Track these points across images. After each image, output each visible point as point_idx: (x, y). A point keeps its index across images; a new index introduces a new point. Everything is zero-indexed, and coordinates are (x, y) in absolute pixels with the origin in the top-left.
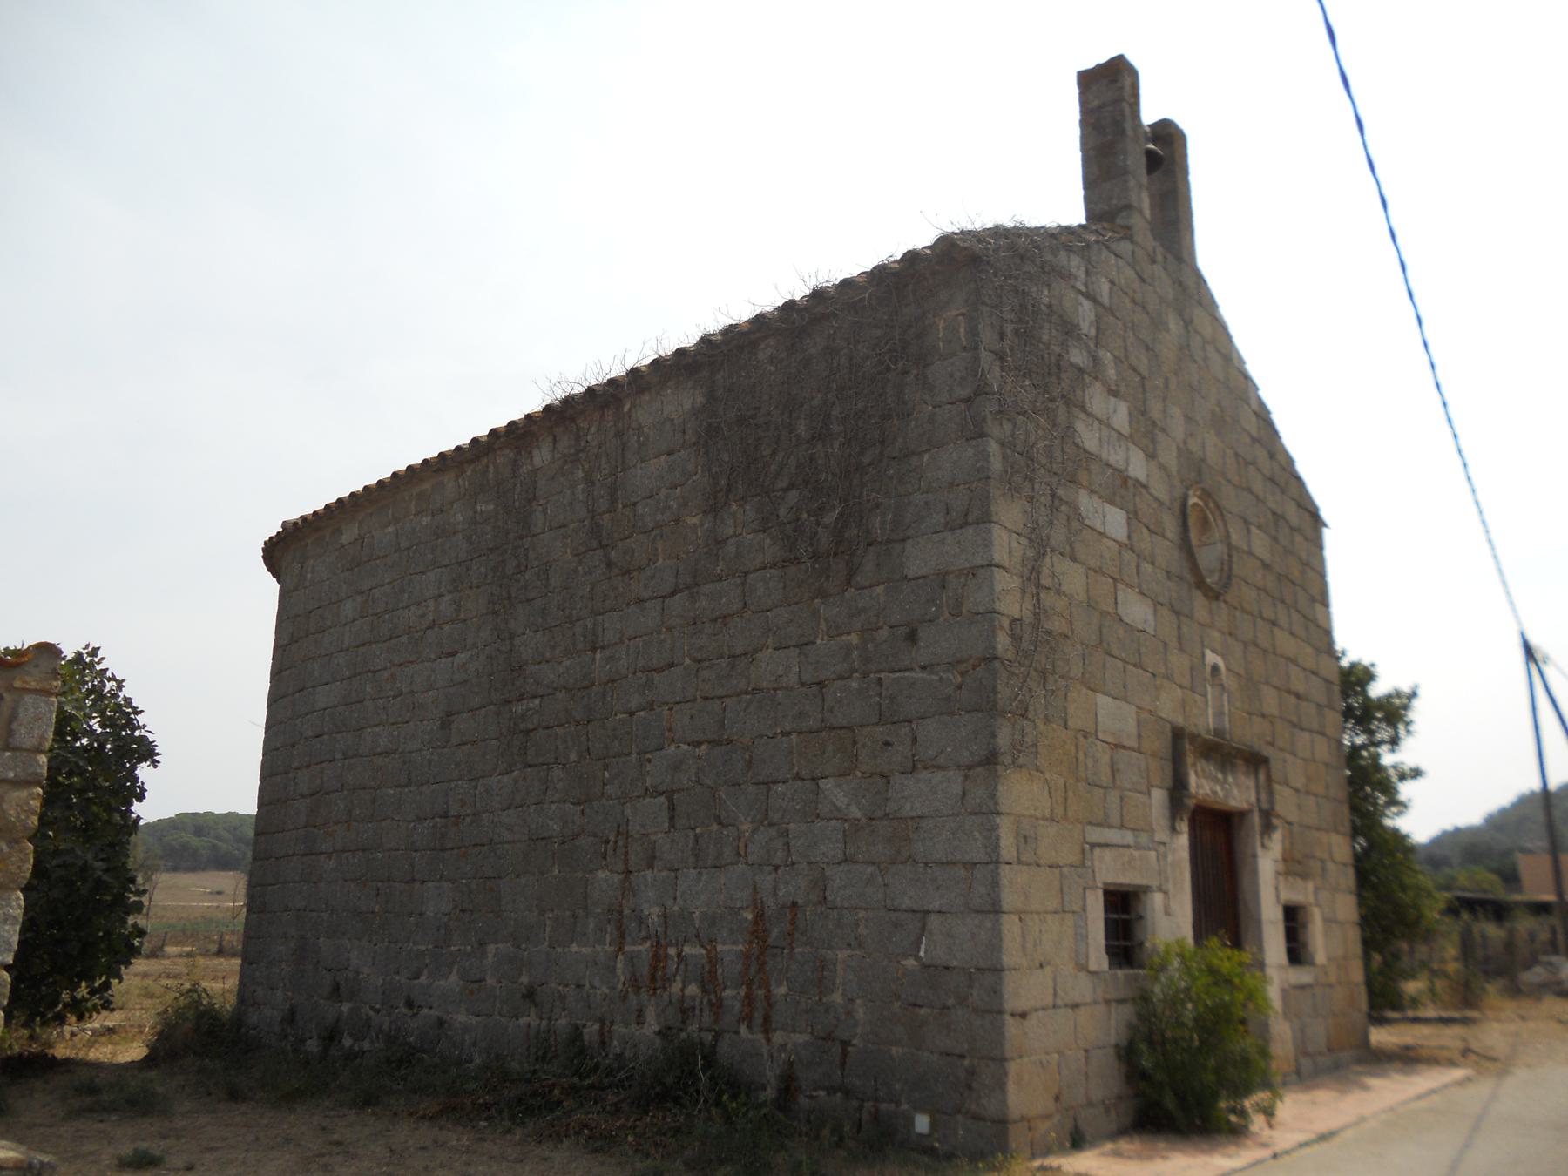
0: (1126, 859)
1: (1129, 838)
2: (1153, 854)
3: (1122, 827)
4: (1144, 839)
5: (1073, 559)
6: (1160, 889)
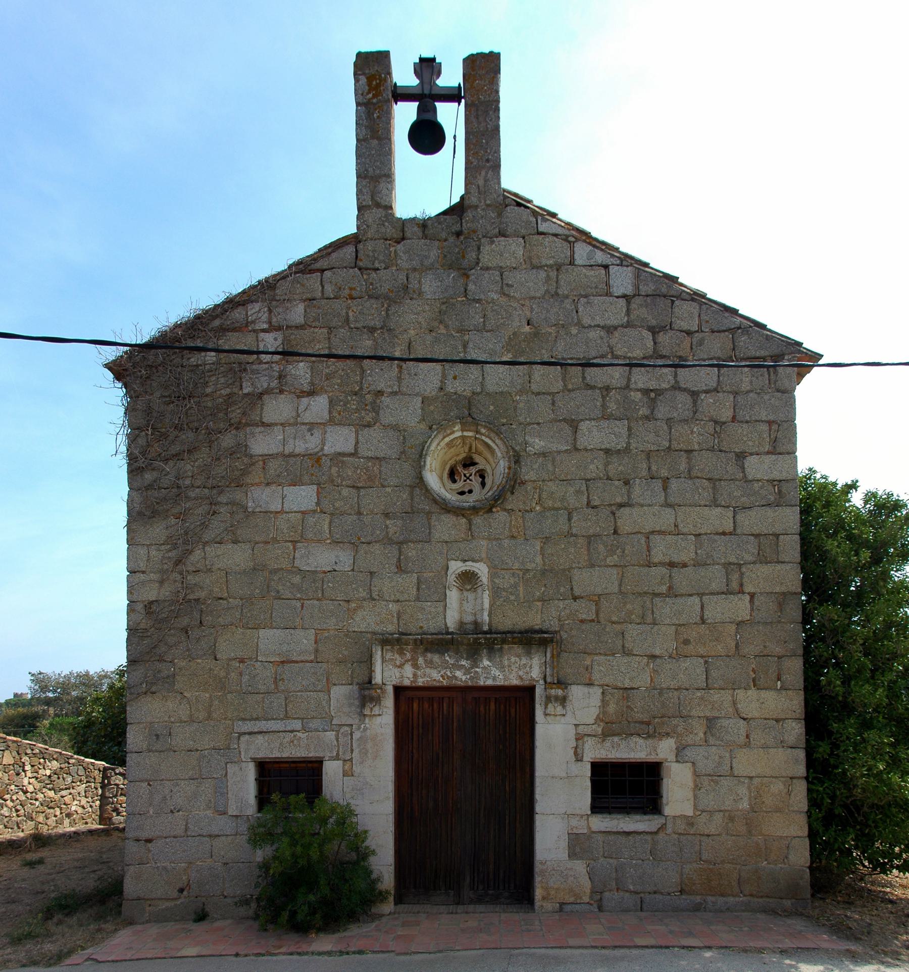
0: (287, 739)
1: (297, 725)
2: (331, 735)
3: (287, 717)
4: (314, 724)
5: (235, 542)
6: (337, 758)
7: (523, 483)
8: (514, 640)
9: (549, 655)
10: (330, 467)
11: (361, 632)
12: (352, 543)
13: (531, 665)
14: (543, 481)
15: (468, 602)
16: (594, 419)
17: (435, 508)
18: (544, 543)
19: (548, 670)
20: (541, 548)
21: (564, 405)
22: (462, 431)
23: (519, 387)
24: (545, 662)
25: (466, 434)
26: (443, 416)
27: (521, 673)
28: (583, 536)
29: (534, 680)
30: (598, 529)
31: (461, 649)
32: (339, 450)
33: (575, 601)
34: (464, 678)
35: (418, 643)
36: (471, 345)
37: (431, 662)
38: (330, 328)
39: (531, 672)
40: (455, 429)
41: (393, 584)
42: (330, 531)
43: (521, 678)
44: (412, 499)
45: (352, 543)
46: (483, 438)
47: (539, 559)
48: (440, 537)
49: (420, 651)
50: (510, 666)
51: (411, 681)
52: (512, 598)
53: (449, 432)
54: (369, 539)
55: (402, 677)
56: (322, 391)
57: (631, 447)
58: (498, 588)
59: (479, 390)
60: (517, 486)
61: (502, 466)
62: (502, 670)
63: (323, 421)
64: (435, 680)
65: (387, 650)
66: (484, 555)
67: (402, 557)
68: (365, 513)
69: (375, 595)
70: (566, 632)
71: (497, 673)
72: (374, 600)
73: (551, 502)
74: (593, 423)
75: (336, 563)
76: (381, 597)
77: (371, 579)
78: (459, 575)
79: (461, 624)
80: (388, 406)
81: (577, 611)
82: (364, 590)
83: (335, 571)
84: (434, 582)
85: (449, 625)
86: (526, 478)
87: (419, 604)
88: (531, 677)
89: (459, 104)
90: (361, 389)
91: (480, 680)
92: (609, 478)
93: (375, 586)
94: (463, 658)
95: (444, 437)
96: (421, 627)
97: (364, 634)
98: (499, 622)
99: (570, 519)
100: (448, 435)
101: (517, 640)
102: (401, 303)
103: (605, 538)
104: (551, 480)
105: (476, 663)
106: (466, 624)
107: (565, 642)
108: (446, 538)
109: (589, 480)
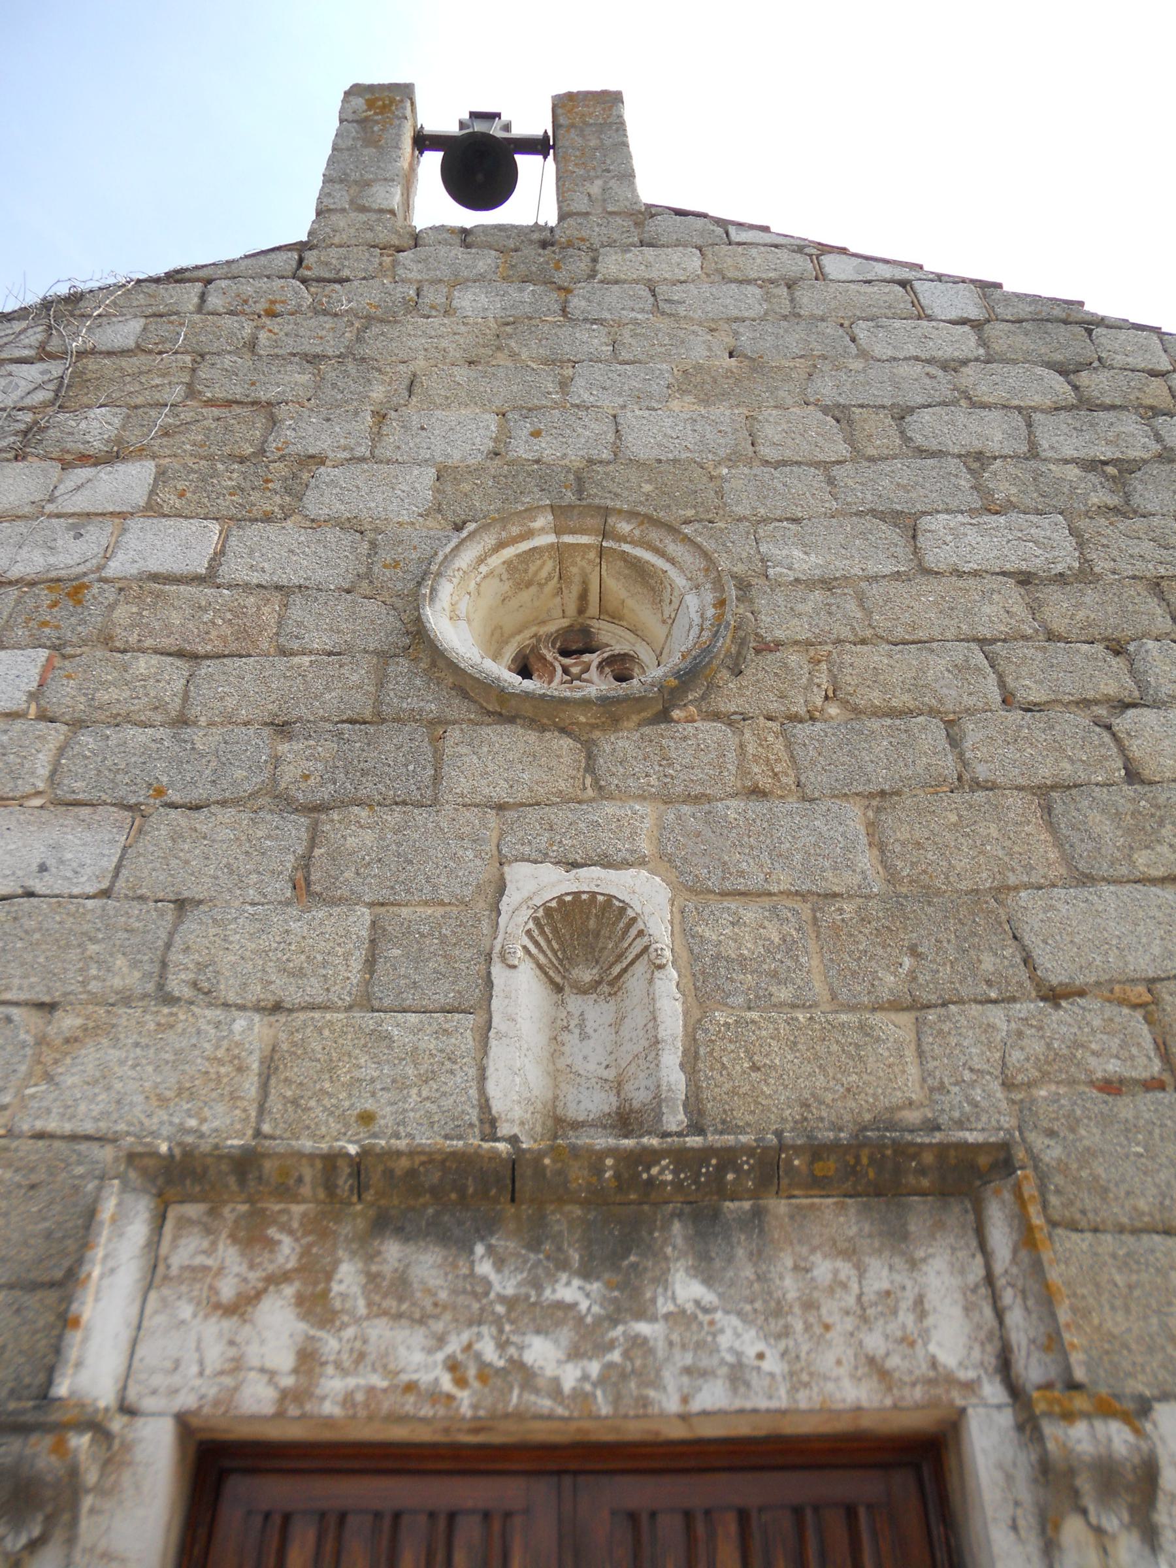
7: (766, 647)
8: (819, 1169)
9: (1001, 1238)
10: (112, 607)
11: (74, 1138)
12: (129, 808)
13: (919, 1301)
14: (838, 641)
15: (584, 1036)
16: (962, 512)
17: (459, 709)
18: (878, 810)
19: (1015, 1317)
20: (871, 825)
21: (861, 484)
22: (558, 532)
23: (722, 453)
24: (990, 1279)
25: (568, 539)
26: (499, 504)
27: (874, 1342)
28: (1020, 788)
29: (950, 1380)
30: (1066, 765)
31: (558, 1220)
32: (154, 566)
33: (1057, 1006)
34: (570, 1377)
35: (344, 1183)
36: (580, 382)
37: (401, 1285)
38: (202, 356)
39: (925, 1334)
40: (540, 523)
41: (264, 942)
42: (54, 772)
43: (876, 1367)
44: (380, 685)
45: (129, 808)
46: (626, 547)
47: (866, 860)
48: (474, 790)
49: (346, 1229)
50: (809, 1305)
51: (284, 1395)
52: (783, 994)
53: (515, 530)
54: (197, 794)
55: (237, 1366)
56: (141, 453)
57: (1097, 570)
58: (718, 957)
59: (606, 455)
60: (751, 655)
61: (692, 610)
62: (775, 1326)
63: (124, 509)
64: (410, 1387)
65: (184, 1223)
66: (646, 847)
67: (317, 852)
68: (203, 721)
69: (177, 984)
70: (1051, 1133)
71: (750, 1343)
72: (170, 1000)
73: (876, 694)
74: (965, 519)
75: (43, 868)
76: (206, 994)
77: (176, 926)
78: (549, 912)
79: (559, 1124)
80: (333, 483)
81: (1077, 1044)
82: (135, 964)
83: (31, 894)
84: (443, 940)
85: (497, 1107)
86: (780, 634)
87: (368, 1020)
88: (934, 1363)
89: (545, 158)
90: (262, 452)
91: (656, 1383)
92: (1052, 637)
93: (187, 950)
94: (563, 1265)
95: (501, 545)
96: (367, 1118)
97: (83, 1147)
98: (734, 1092)
99: (954, 742)
100: (514, 541)
101: (829, 1166)
102: (396, 322)
103: (1101, 794)
104: (863, 642)
105: (635, 1293)
106: (576, 1125)
107: (1059, 1179)
108: (500, 793)
109: (994, 641)
